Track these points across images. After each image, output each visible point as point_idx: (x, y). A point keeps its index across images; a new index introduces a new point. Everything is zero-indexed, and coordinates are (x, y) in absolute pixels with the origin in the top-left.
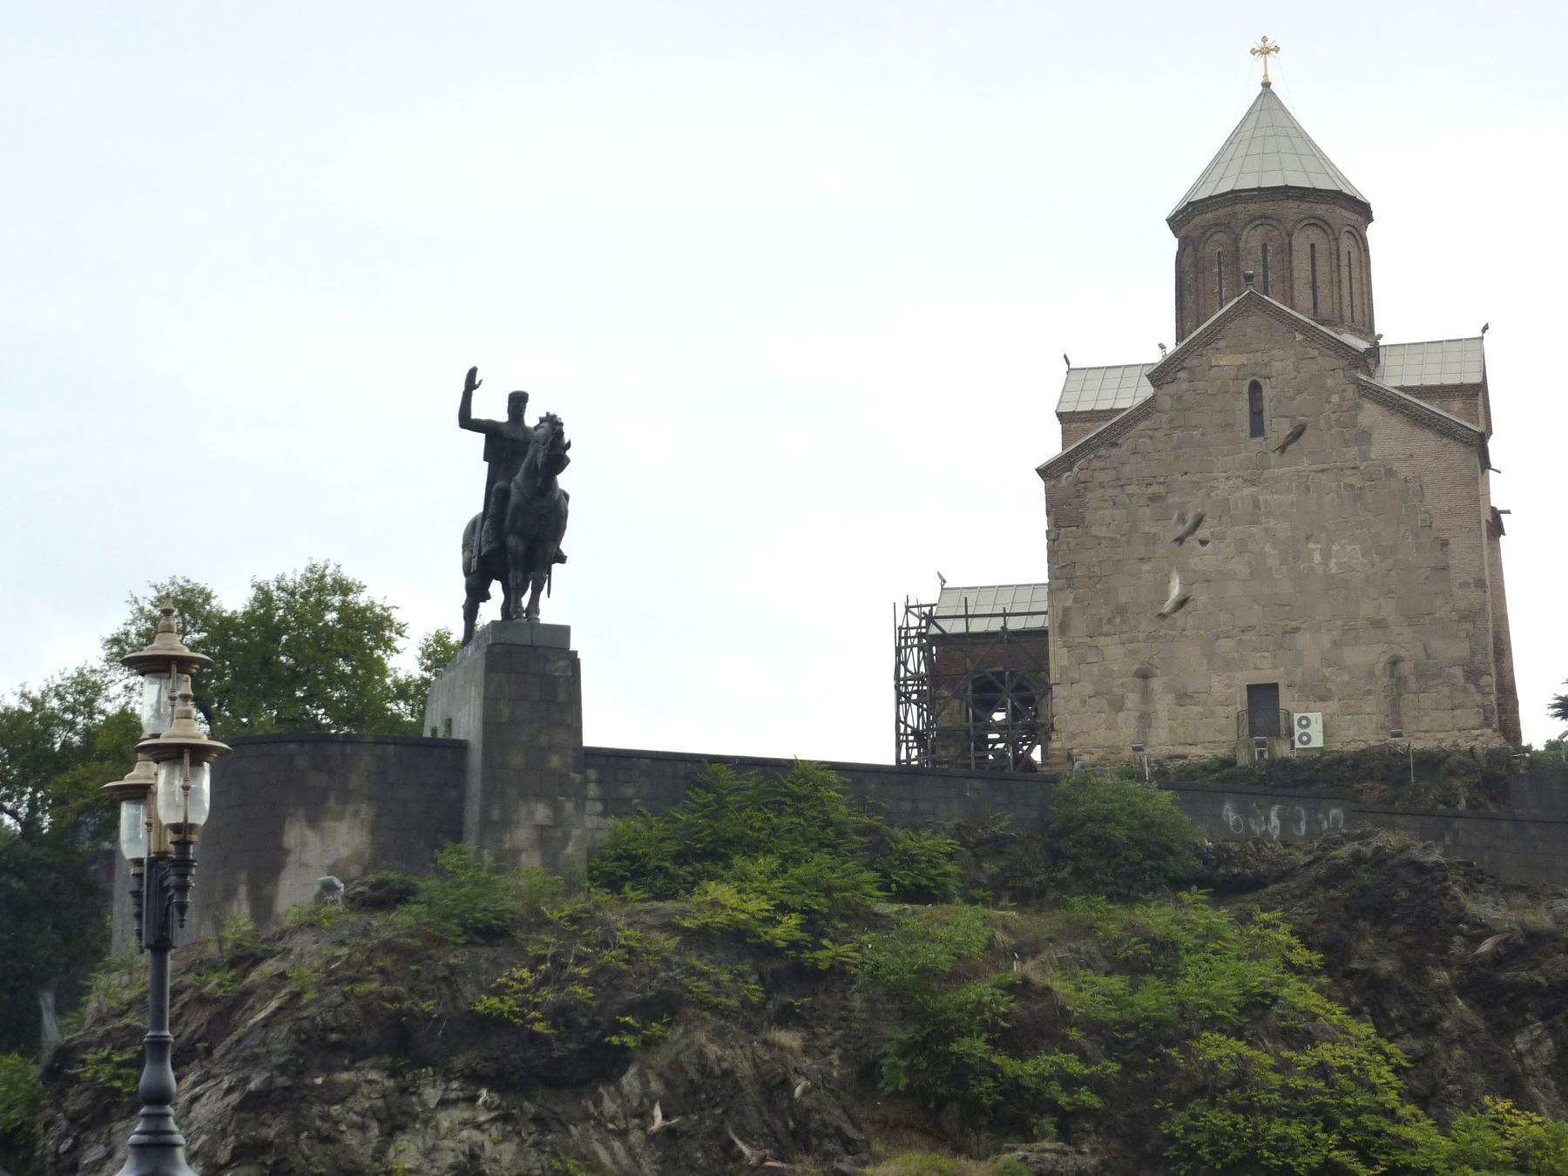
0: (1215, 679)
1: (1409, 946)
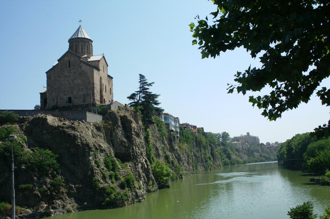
0: (65, 97)
1: (41, 128)
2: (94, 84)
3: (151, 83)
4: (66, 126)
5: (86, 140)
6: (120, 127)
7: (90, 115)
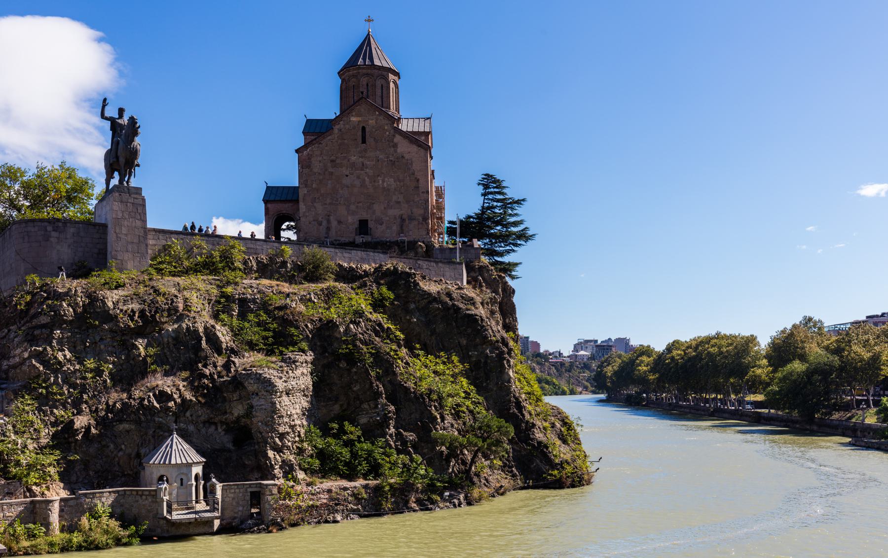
0: (349, 218)
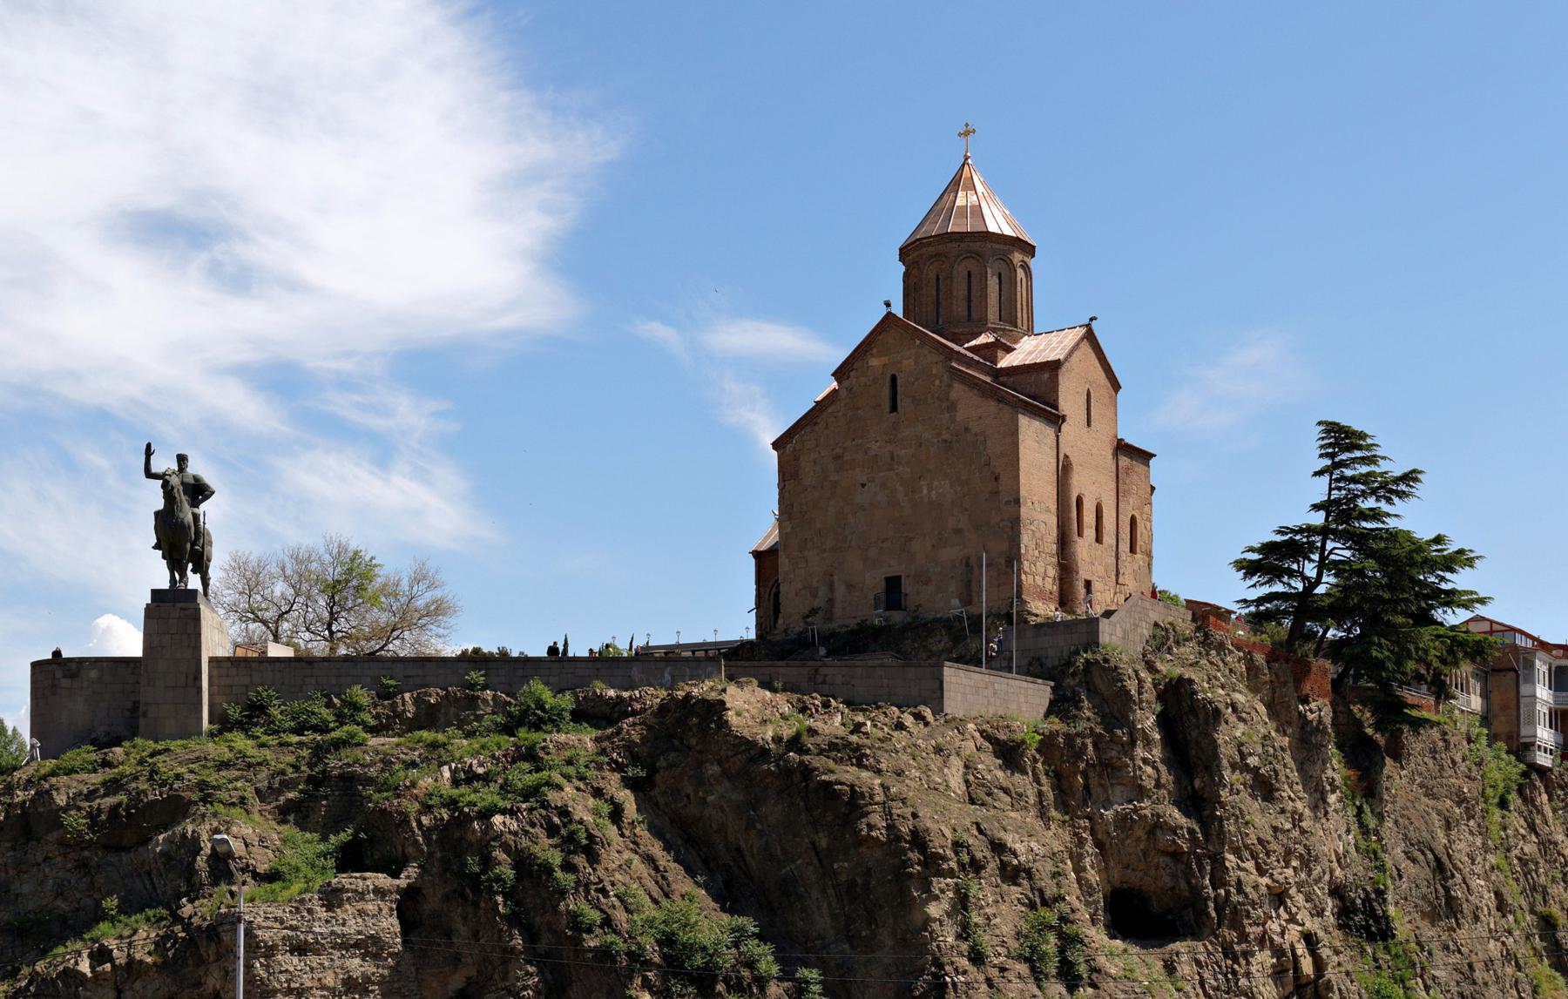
2: (1017, 502)
3: (1397, 480)
4: (818, 740)
5: (915, 816)
6: (1148, 743)
7: (965, 681)
